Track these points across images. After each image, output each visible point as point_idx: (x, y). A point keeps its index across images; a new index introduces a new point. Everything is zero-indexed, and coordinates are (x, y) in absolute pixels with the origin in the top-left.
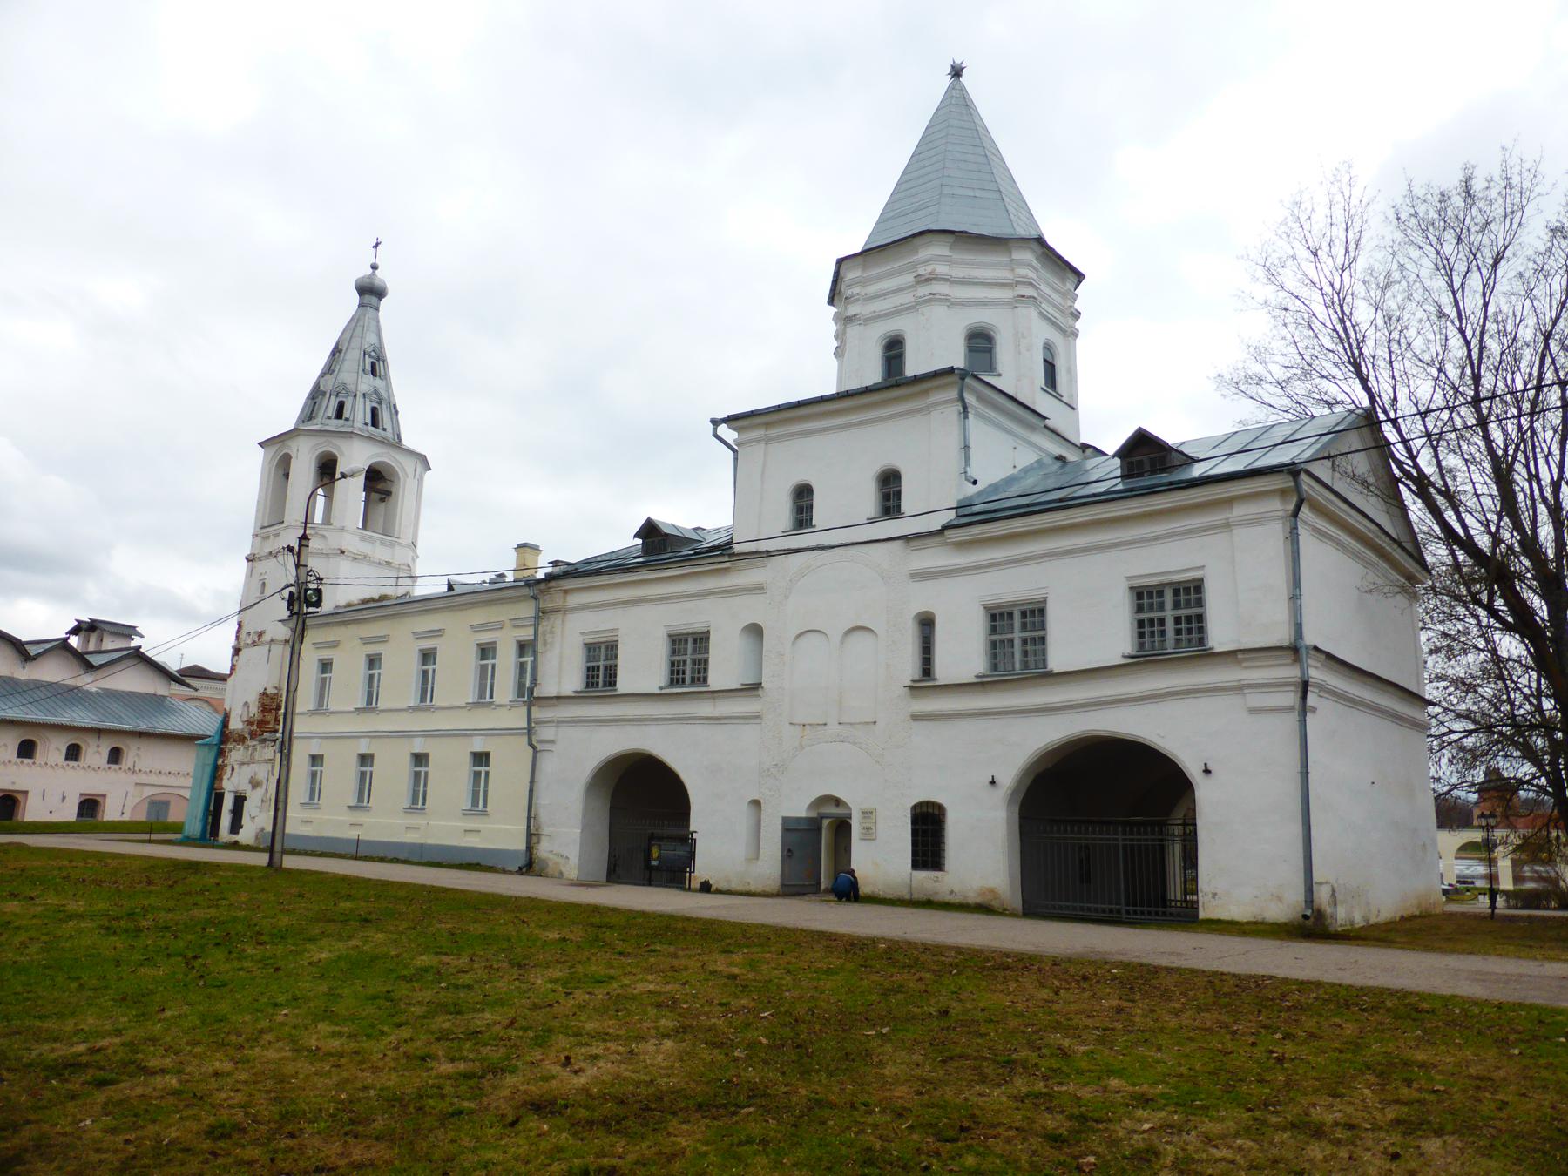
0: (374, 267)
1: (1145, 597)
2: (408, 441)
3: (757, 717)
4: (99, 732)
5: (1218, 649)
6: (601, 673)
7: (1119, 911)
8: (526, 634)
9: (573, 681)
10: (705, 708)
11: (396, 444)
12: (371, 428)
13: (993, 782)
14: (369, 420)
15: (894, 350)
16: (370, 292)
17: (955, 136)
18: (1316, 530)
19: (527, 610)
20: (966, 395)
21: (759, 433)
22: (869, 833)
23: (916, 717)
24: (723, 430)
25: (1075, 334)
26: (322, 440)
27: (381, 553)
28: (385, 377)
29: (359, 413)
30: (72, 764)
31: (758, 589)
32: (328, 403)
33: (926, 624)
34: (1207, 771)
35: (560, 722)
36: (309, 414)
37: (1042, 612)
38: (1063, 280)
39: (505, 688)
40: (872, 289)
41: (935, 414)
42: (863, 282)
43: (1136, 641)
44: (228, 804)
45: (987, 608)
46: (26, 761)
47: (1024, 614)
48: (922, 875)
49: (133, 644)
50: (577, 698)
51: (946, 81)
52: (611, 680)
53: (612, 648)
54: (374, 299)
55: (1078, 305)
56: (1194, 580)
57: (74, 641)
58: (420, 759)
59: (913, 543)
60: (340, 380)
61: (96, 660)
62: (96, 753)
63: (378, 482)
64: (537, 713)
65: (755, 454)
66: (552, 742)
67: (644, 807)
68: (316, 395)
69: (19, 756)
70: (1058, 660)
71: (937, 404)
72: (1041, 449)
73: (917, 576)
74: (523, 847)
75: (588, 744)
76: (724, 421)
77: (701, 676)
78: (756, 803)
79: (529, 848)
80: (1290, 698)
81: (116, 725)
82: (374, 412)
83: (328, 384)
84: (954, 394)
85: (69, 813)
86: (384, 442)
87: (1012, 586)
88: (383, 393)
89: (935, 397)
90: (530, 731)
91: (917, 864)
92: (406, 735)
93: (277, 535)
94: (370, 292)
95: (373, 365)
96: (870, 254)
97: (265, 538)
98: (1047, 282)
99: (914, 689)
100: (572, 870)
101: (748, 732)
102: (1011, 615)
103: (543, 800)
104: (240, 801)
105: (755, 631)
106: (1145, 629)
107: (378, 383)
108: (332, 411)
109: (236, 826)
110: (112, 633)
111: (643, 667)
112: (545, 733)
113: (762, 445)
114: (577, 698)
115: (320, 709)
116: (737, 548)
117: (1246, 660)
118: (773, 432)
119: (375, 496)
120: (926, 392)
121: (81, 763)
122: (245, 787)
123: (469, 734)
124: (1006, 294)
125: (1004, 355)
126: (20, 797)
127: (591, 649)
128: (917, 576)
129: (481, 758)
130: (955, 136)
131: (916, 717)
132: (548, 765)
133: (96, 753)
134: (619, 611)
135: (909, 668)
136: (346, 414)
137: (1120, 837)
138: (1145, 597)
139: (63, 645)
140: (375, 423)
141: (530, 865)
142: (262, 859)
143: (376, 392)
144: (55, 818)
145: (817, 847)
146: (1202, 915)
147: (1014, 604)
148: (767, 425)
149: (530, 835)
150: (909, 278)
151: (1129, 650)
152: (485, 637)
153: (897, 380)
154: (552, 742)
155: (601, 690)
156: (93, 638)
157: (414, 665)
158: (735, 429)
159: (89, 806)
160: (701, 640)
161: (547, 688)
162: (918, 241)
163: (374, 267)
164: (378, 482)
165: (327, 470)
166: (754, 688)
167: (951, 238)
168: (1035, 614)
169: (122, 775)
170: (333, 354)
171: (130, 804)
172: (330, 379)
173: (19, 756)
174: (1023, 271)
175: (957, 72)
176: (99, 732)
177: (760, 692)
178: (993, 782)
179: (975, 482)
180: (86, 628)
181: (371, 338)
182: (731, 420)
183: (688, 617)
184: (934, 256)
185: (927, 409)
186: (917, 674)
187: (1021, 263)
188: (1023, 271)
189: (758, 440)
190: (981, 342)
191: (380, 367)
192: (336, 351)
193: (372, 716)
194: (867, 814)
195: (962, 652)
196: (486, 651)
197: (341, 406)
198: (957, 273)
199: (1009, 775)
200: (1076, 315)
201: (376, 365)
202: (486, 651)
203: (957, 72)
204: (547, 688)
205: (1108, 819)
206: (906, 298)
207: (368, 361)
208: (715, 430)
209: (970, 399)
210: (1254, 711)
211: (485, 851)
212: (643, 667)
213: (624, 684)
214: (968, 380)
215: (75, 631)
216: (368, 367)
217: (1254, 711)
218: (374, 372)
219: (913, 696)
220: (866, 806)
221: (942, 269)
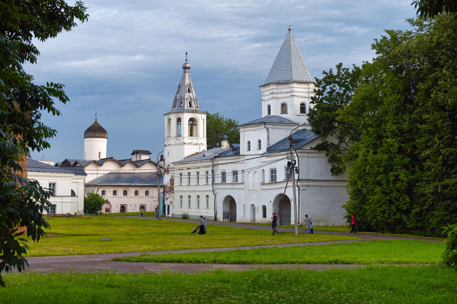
0: (186, 60)
10: (237, 187)
12: (190, 108)
22: (258, 212)
23: (262, 189)
27: (195, 141)
30: (137, 196)
35: (218, 189)
46: (126, 196)
70: (277, 181)
75: (222, 194)
77: (237, 181)
82: (190, 103)
84: (264, 126)
85: (137, 210)
92: (195, 191)
101: (243, 191)
104: (169, 206)
109: (169, 213)
111: (229, 179)
112: (216, 191)
115: (181, 185)
118: (245, 129)
123: (206, 191)
125: (289, 109)
126: (125, 206)
132: (218, 198)
140: (190, 106)
143: (190, 97)
144: (135, 211)
156: (138, 155)
159: (142, 207)
166: (243, 183)
169: (149, 198)
171: (153, 206)
172: (178, 95)
176: (142, 186)
193: (189, 187)
198: (279, 91)
213: (227, 182)
215: (133, 154)
216: (187, 91)
221: (275, 91)
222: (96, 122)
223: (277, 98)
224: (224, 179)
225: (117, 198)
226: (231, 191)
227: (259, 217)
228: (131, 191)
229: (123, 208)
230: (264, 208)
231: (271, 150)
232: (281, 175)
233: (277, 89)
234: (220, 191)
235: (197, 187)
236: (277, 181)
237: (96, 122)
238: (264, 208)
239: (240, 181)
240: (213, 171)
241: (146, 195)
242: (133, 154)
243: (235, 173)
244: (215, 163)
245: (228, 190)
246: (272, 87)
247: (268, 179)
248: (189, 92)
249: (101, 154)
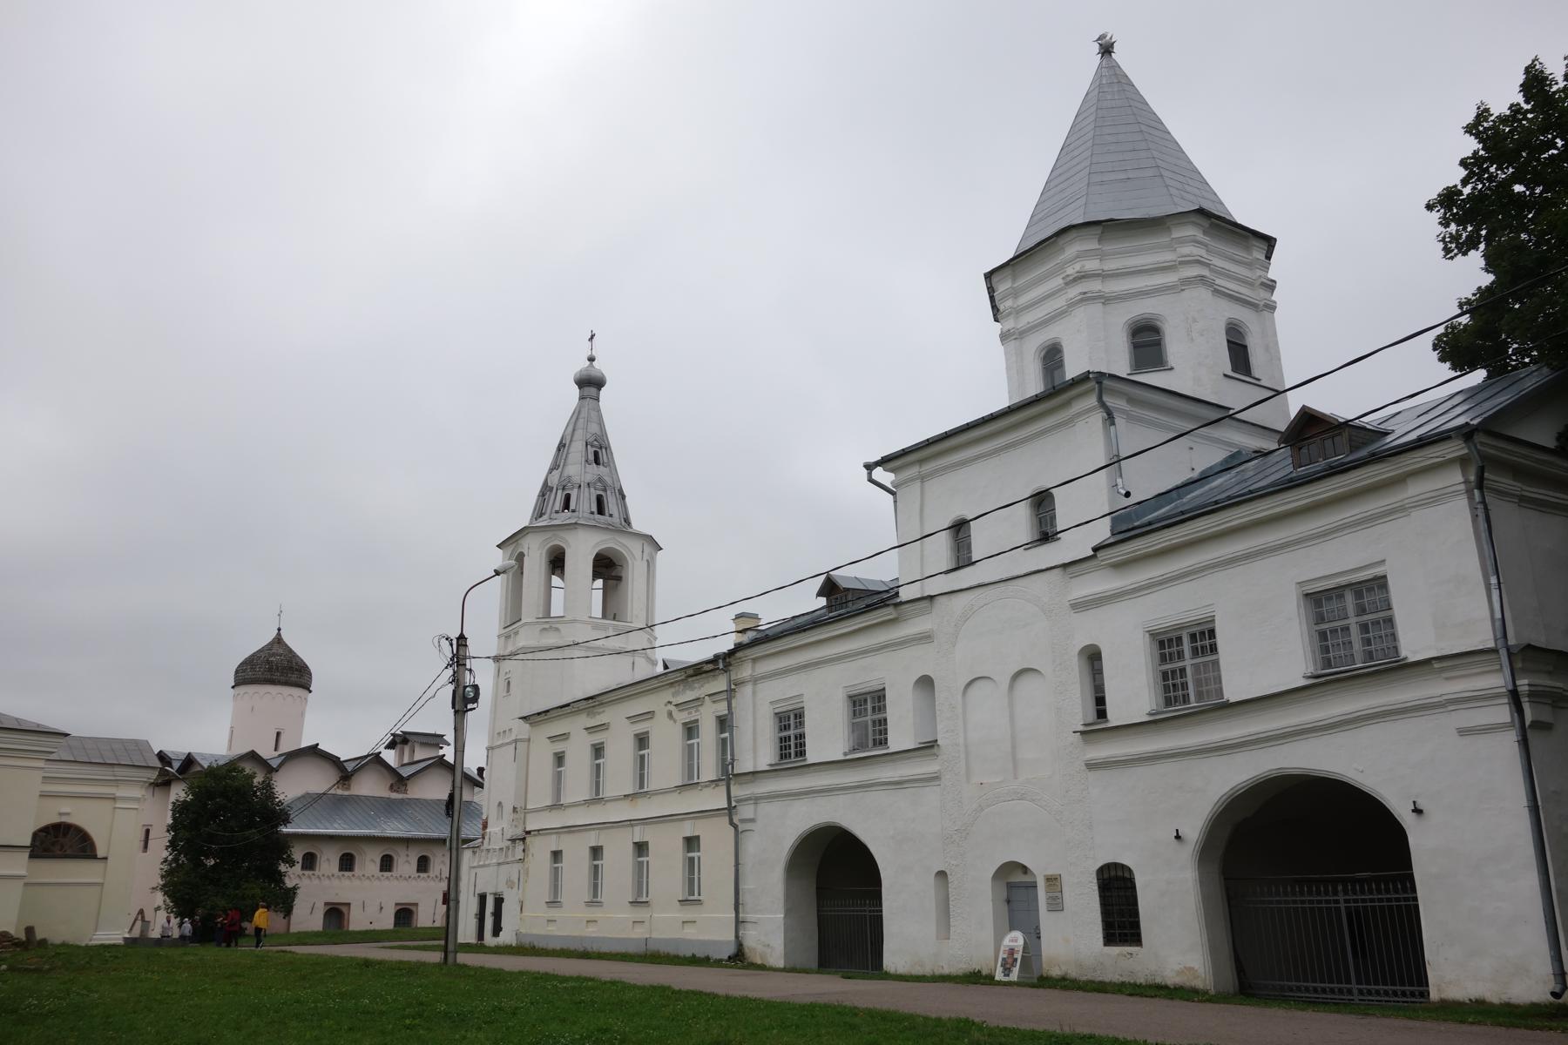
0: (591, 359)
1: (1319, 601)
2: (638, 525)
3: (934, 778)
4: (408, 842)
5: (1412, 659)
6: (791, 746)
7: (1350, 992)
8: (722, 708)
9: (766, 756)
13: (1178, 837)
14: (594, 509)
15: (1052, 357)
16: (590, 384)
17: (1116, 116)
18: (1523, 501)
19: (720, 684)
20: (1105, 398)
21: (913, 471)
22: (1056, 905)
23: (1092, 766)
24: (879, 474)
25: (1272, 307)
26: (549, 535)
28: (610, 464)
29: (584, 503)
30: (387, 874)
31: (926, 638)
32: (556, 496)
33: (1093, 657)
34: (1417, 811)
35: (756, 800)
36: (539, 513)
37: (1212, 633)
38: (1248, 249)
39: (709, 769)
40: (1024, 300)
41: (1080, 425)
42: (1015, 294)
43: (1319, 656)
44: (490, 907)
45: (1153, 635)
46: (347, 874)
47: (1193, 637)
48: (1115, 950)
49: (441, 752)
50: (773, 771)
51: (1097, 59)
52: (801, 753)
53: (799, 716)
54: (592, 390)
55: (1272, 274)
56: (1376, 578)
57: (390, 757)
59: (1070, 570)
60: (566, 474)
61: (405, 772)
62: (406, 863)
63: (607, 567)
64: (736, 791)
65: (911, 494)
66: (752, 820)
68: (546, 489)
69: (341, 869)
71: (1079, 415)
72: (1229, 444)
73: (1080, 606)
74: (732, 937)
76: (878, 464)
77: (883, 742)
78: (942, 875)
79: (737, 936)
80: (1502, 713)
81: (421, 834)
82: (600, 500)
83: (554, 480)
84: (1092, 401)
85: (387, 922)
86: (608, 528)
87: (1176, 605)
88: (608, 480)
89: (1078, 407)
90: (730, 810)
91: (1110, 939)
92: (631, 823)
93: (516, 633)
94: (590, 384)
95: (596, 454)
96: (1022, 259)
97: (508, 637)
98: (1224, 258)
99: (1087, 734)
100: (777, 958)
101: (931, 795)
102: (1179, 639)
103: (747, 885)
104: (499, 901)
105: (926, 683)
106: (1325, 640)
107: (602, 470)
108: (558, 505)
109: (497, 930)
110: (423, 744)
111: (827, 737)
112: (745, 811)
113: (918, 484)
114: (773, 771)
116: (905, 594)
117: (1442, 670)
119: (611, 582)
120: (1068, 403)
121: (394, 873)
122: (501, 888)
124: (1171, 278)
125: (1175, 347)
126: (344, 909)
128: (1080, 606)
130: (1116, 116)
131: (1092, 766)
132: (751, 846)
133: (406, 863)
134: (802, 677)
135: (1078, 711)
136: (572, 506)
137: (1341, 897)
138: (1319, 601)
139: (376, 759)
140: (601, 511)
141: (739, 958)
142: (437, 957)
143: (600, 480)
144: (377, 926)
146: (1434, 995)
147: (1181, 627)
148: (921, 462)
149: (739, 922)
150: (1058, 281)
151: (1311, 670)
153: (1057, 391)
154: (752, 820)
155: (793, 761)
156: (407, 750)
158: (892, 471)
159: (404, 914)
160: (879, 697)
161: (745, 765)
162: (1062, 241)
163: (591, 359)
164: (607, 567)
165: (557, 563)
166: (930, 747)
167: (1098, 230)
168: (1204, 638)
170: (559, 449)
172: (556, 473)
173: (341, 869)
174: (1188, 250)
175: (1107, 49)
177: (935, 750)
178: (1178, 837)
179: (1128, 495)
180: (399, 741)
181: (594, 428)
182: (884, 462)
183: (863, 674)
184: (1077, 255)
185: (1069, 422)
186: (1092, 716)
187: (1182, 241)
188: (1188, 250)
189: (912, 480)
190: (1147, 342)
191: (603, 456)
192: (561, 446)
194: (1052, 881)
195: (1134, 691)
196: (691, 730)
197: (568, 498)
198: (1111, 265)
199: (1194, 830)
200: (1270, 286)
201: (599, 453)
202: (691, 730)
203: (1107, 49)
204: (745, 765)
205: (1313, 875)
206: (1059, 303)
207: (591, 450)
208: (870, 474)
209: (1110, 401)
210: (1463, 732)
211: (704, 943)
212: (827, 737)
213: (812, 756)
214: (1106, 382)
215: (391, 746)
216: (591, 457)
217: (1463, 732)
218: (597, 461)
219: (1086, 742)
220: (1050, 872)
221: (1092, 265)
222: (278, 640)
223: (1106, 300)
224: (791, 746)
225: (316, 882)
226: (842, 800)
227: (1073, 936)
228: (368, 862)
229: (335, 913)
230: (1117, 889)
231: (1136, 528)
233: (1102, 257)
234: (766, 808)
235: (641, 802)
236: (1232, 693)
237: (278, 640)
238: (1117, 889)
239: (900, 737)
240: (724, 723)
241: (419, 870)
242: (391, 746)
243: (868, 707)
244: (745, 671)
245: (821, 802)
246: (1073, 248)
248: (597, 461)
249: (282, 737)
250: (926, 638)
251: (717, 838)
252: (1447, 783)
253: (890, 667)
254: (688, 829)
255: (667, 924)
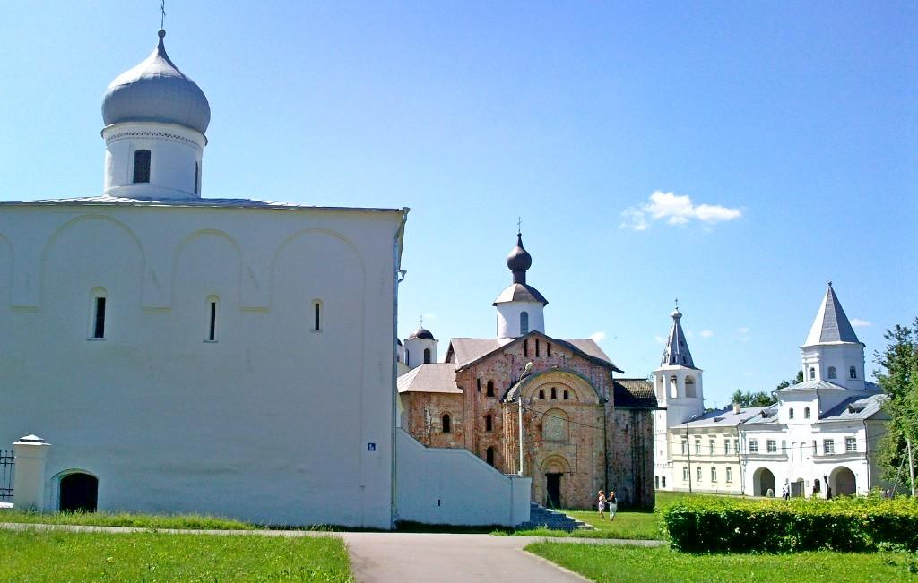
11: (692, 367)
23: (816, 463)
39: (732, 451)
58: (714, 468)
67: (765, 481)
75: (752, 467)
87: (828, 436)
104: (664, 478)
127: (751, 443)
128: (814, 433)
129: (729, 468)
145: (797, 487)
152: (727, 438)
157: (708, 444)
196: (727, 441)
201: (683, 343)
202: (727, 441)
203: (830, 284)
213: (760, 452)
232: (840, 448)
238: (817, 483)
247: (821, 451)
250: (785, 432)
251: (735, 468)
252: (860, 470)
253: (778, 437)
254: (728, 465)
255: (721, 486)
